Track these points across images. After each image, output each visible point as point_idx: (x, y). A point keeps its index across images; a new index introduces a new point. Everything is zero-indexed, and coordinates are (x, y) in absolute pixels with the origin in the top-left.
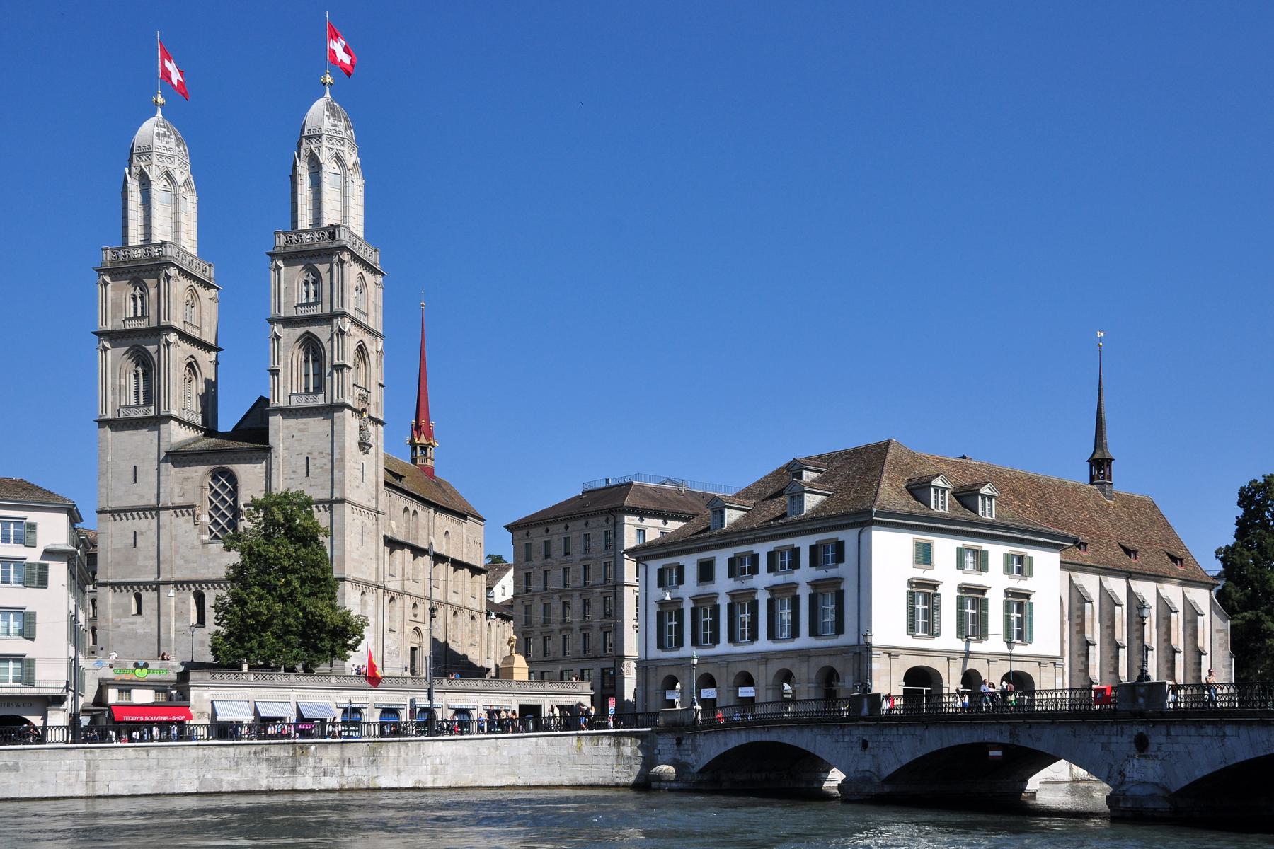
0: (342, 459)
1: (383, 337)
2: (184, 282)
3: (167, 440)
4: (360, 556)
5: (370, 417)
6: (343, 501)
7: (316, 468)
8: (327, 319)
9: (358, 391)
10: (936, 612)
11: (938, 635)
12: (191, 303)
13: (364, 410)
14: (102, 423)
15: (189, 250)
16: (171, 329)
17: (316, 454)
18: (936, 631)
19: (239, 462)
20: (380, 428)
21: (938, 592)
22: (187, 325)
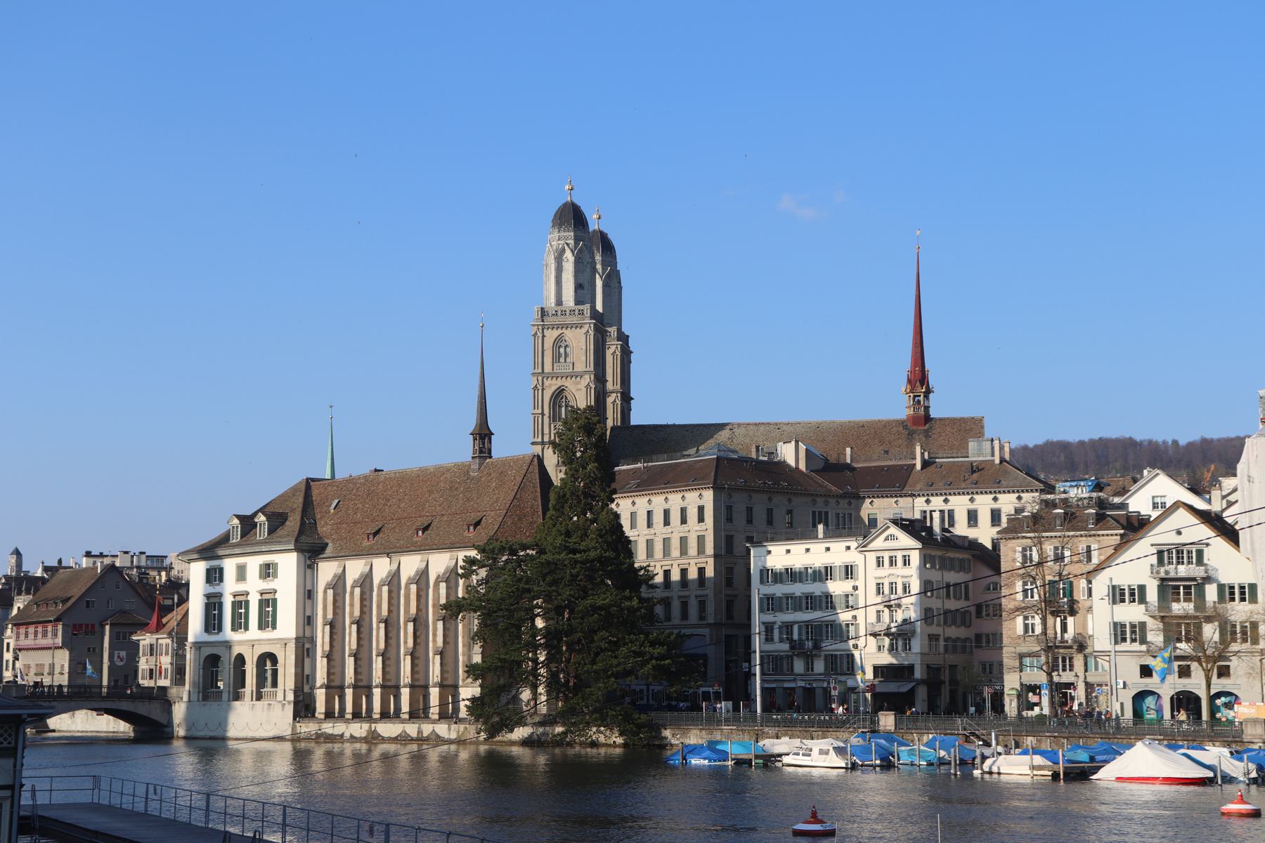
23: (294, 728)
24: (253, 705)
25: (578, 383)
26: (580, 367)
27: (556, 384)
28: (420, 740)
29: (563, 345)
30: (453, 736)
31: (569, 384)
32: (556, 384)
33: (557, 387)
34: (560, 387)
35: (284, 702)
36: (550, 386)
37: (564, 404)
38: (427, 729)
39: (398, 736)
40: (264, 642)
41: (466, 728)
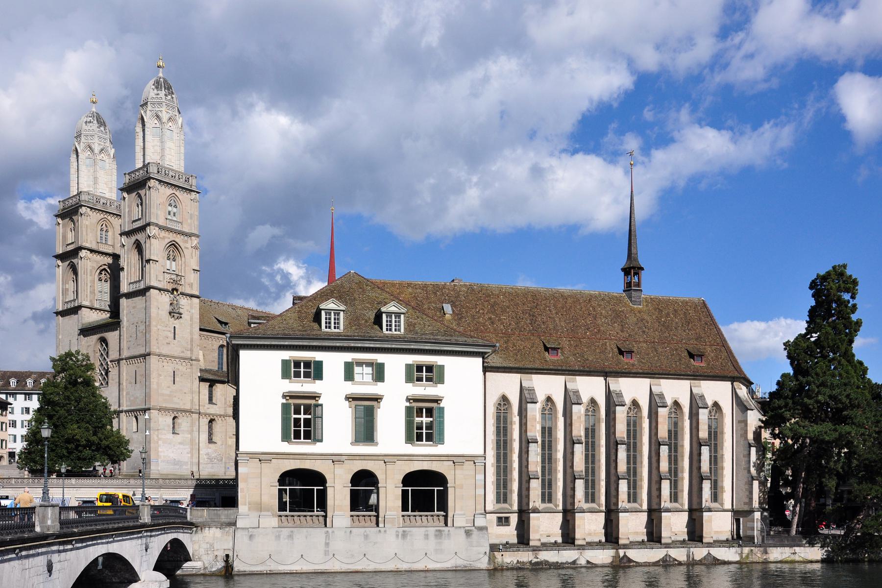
0: (149, 325)
1: (197, 236)
2: (96, 216)
3: (81, 322)
4: (171, 392)
5: (182, 294)
6: (149, 354)
7: (140, 333)
8: (143, 229)
9: (167, 276)
10: (318, 421)
11: (321, 441)
12: (105, 229)
13: (173, 290)
14: (58, 313)
15: (107, 195)
16: (81, 248)
17: (139, 322)
18: (318, 437)
19: (109, 331)
20: (196, 301)
21: (320, 402)
22: (100, 244)
23: (492, 559)
24: (404, 531)
25: (186, 242)
26: (186, 229)
27: (169, 238)
28: (691, 563)
29: (173, 205)
30: (737, 558)
31: (179, 239)
32: (169, 238)
33: (167, 241)
34: (171, 242)
35: (467, 528)
36: (164, 238)
37: (171, 257)
38: (699, 553)
39: (659, 561)
40: (421, 458)
41: (752, 550)
